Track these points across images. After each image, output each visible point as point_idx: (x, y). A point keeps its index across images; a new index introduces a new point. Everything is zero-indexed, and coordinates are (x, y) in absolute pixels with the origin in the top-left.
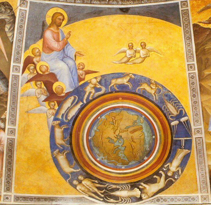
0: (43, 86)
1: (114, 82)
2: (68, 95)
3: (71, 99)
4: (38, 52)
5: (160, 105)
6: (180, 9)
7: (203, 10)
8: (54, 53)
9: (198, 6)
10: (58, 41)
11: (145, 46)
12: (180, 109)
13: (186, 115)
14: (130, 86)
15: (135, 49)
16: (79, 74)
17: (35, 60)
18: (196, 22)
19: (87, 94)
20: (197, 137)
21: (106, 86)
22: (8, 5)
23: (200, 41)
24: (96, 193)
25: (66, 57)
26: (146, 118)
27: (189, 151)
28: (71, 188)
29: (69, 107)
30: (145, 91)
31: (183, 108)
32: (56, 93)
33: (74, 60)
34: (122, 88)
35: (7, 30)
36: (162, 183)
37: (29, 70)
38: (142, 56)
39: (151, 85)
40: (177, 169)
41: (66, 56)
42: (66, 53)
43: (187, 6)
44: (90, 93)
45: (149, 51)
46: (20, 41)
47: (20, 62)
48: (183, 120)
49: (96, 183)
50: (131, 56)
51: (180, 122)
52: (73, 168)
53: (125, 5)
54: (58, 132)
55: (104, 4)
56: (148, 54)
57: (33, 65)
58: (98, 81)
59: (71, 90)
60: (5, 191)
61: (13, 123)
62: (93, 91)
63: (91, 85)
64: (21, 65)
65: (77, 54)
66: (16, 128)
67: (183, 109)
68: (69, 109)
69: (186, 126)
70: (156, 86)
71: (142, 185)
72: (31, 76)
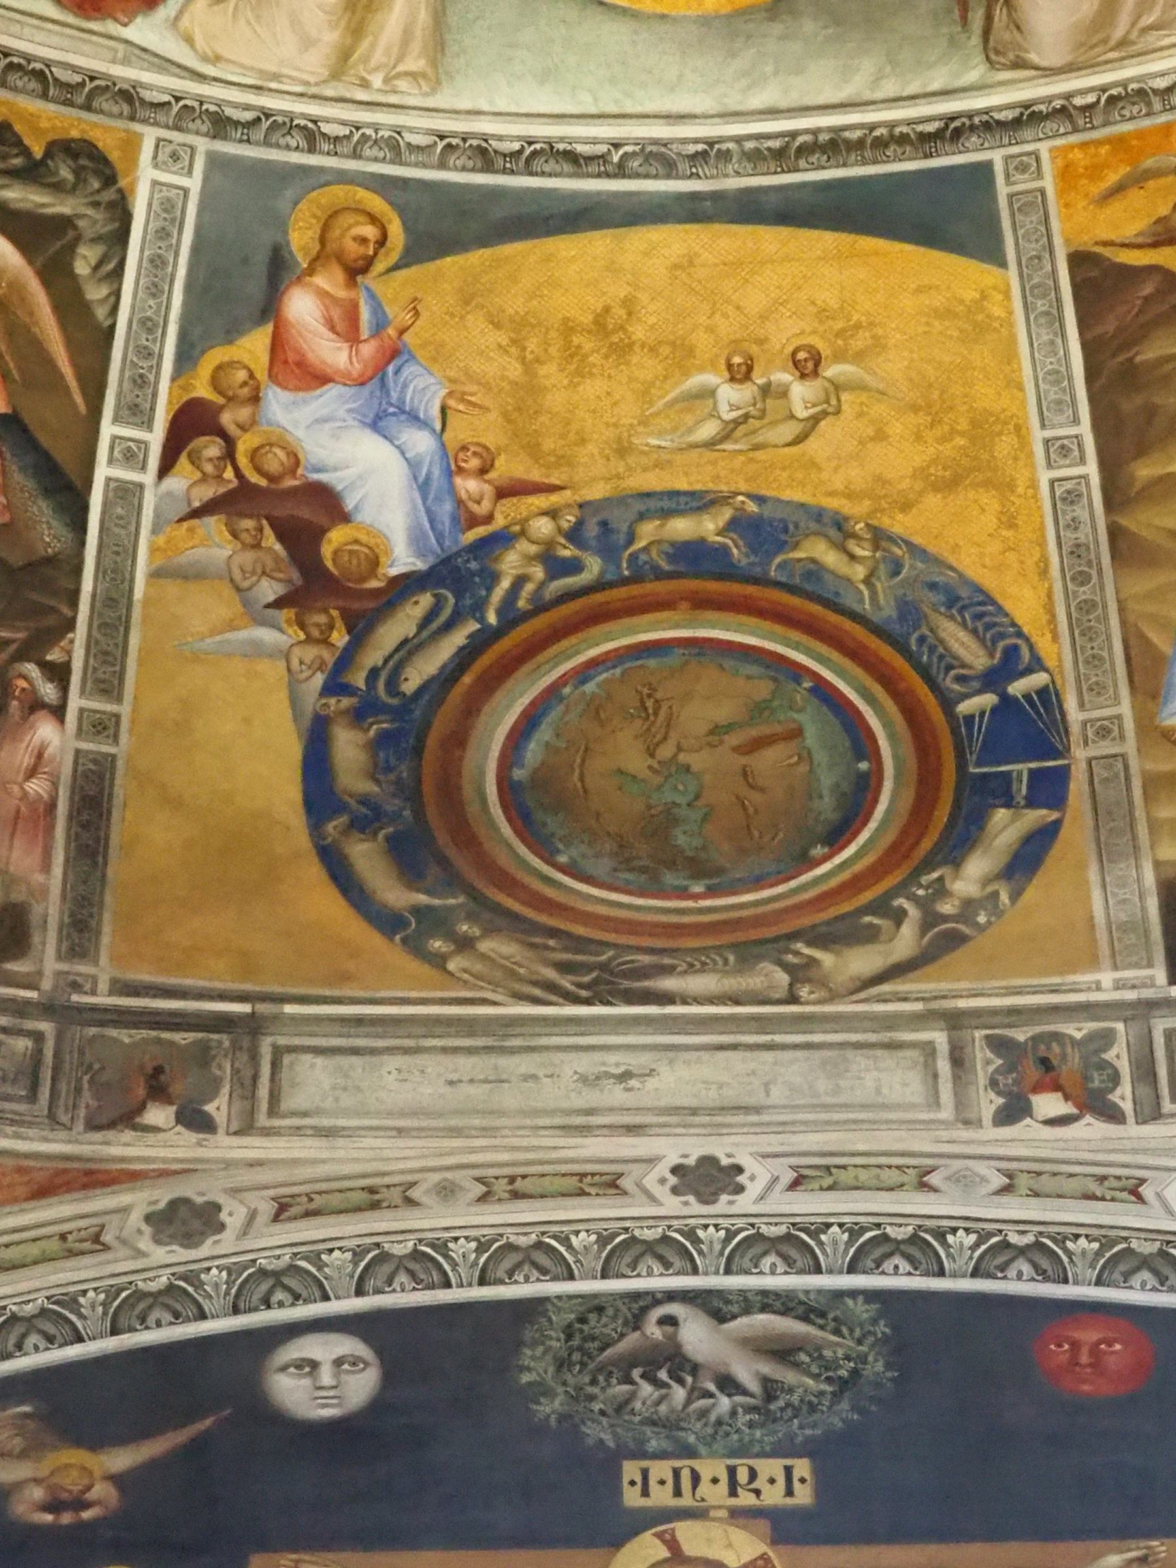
0: (270, 540)
1: (648, 531)
2: (406, 585)
3: (416, 603)
4: (245, 384)
5: (897, 628)
6: (1002, 190)
7: (1119, 189)
8: (332, 392)
9: (1095, 171)
10: (349, 331)
11: (817, 364)
12: (1001, 645)
13: (1037, 664)
14: (737, 546)
15: (761, 381)
16: (464, 495)
17: (226, 419)
18: (1085, 242)
19: (505, 583)
20: (1098, 753)
21: (609, 552)
22: (91, 157)
23: (1109, 326)
24: (551, 987)
25: (394, 414)
26: (824, 693)
27: (1055, 815)
28: (424, 970)
29: (405, 642)
30: (815, 571)
31: (1020, 634)
32: (336, 572)
33: (438, 427)
34: (693, 556)
35: (82, 268)
36: (905, 941)
37: (194, 460)
38: (801, 413)
39: (852, 546)
40: (989, 889)
41: (391, 410)
42: (394, 395)
43: (1039, 174)
44: (520, 581)
45: (837, 387)
46: (150, 325)
47: (149, 425)
48: (1017, 688)
49: (553, 949)
50: (740, 412)
51: (1005, 699)
52: (428, 892)
53: (712, 177)
54: (349, 748)
55: (599, 175)
56: (834, 402)
57: (218, 440)
58: (565, 525)
59: (421, 565)
60: (59, 958)
61: (108, 685)
62: (538, 572)
63: (523, 546)
64: (156, 439)
65: (452, 403)
66: (125, 710)
67: (1019, 642)
68: (408, 649)
69: (1038, 713)
70: (876, 547)
71: (797, 953)
72: (208, 492)
